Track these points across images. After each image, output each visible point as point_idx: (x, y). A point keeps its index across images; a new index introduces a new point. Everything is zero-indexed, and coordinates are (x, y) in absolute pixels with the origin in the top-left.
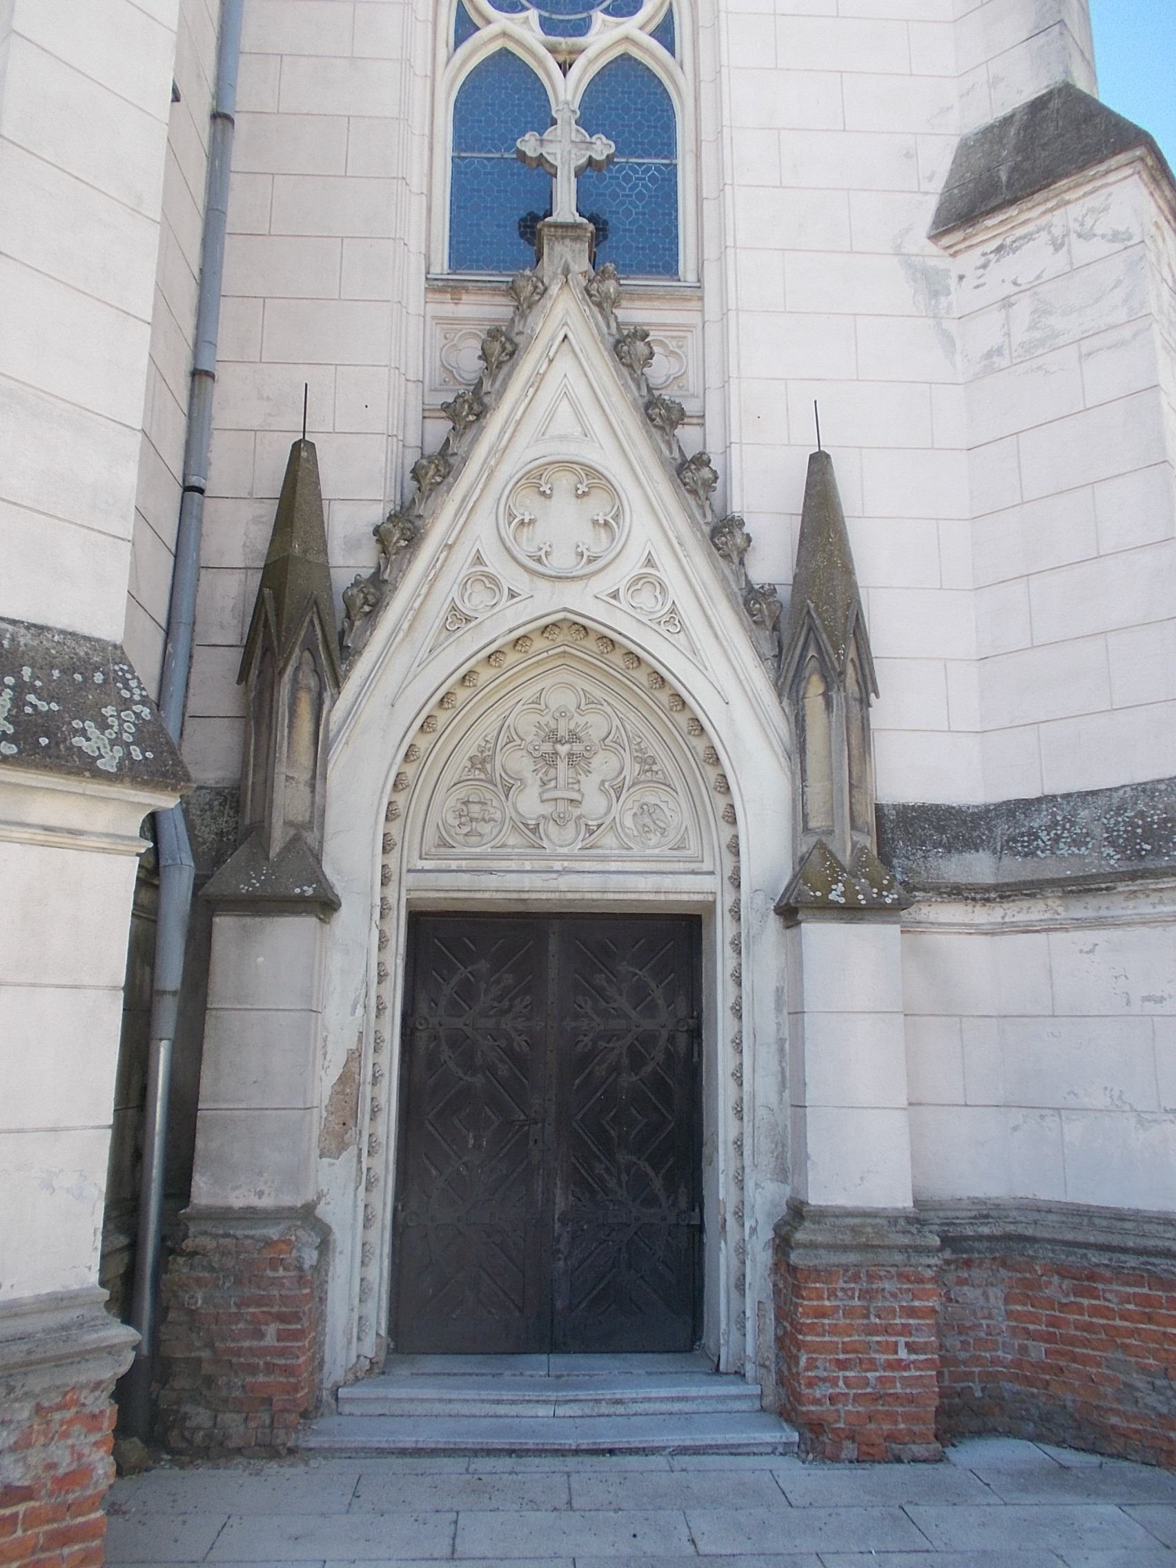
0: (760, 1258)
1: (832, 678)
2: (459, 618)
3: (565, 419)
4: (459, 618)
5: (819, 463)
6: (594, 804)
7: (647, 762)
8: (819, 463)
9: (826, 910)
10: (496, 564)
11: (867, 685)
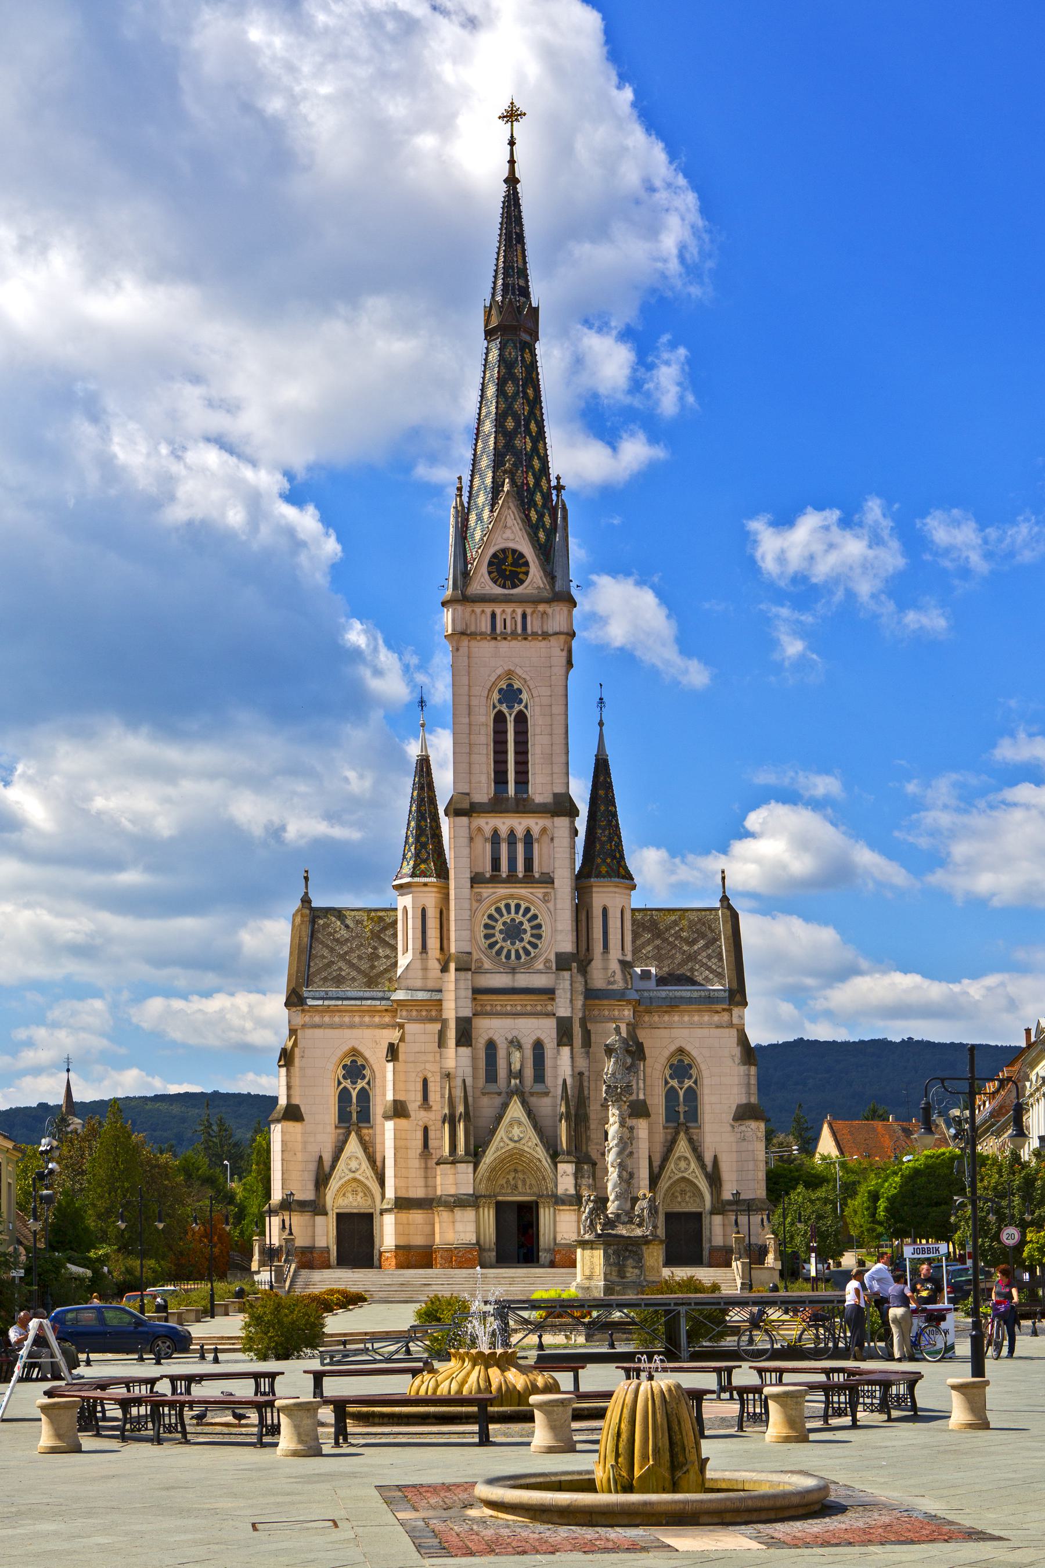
0: (707, 1253)
1: (716, 1186)
2: (670, 1178)
3: (682, 1150)
4: (670, 1178)
5: (715, 1157)
6: (687, 1199)
7: (694, 1194)
8: (715, 1157)
9: (714, 1214)
10: (674, 1170)
11: (721, 1185)
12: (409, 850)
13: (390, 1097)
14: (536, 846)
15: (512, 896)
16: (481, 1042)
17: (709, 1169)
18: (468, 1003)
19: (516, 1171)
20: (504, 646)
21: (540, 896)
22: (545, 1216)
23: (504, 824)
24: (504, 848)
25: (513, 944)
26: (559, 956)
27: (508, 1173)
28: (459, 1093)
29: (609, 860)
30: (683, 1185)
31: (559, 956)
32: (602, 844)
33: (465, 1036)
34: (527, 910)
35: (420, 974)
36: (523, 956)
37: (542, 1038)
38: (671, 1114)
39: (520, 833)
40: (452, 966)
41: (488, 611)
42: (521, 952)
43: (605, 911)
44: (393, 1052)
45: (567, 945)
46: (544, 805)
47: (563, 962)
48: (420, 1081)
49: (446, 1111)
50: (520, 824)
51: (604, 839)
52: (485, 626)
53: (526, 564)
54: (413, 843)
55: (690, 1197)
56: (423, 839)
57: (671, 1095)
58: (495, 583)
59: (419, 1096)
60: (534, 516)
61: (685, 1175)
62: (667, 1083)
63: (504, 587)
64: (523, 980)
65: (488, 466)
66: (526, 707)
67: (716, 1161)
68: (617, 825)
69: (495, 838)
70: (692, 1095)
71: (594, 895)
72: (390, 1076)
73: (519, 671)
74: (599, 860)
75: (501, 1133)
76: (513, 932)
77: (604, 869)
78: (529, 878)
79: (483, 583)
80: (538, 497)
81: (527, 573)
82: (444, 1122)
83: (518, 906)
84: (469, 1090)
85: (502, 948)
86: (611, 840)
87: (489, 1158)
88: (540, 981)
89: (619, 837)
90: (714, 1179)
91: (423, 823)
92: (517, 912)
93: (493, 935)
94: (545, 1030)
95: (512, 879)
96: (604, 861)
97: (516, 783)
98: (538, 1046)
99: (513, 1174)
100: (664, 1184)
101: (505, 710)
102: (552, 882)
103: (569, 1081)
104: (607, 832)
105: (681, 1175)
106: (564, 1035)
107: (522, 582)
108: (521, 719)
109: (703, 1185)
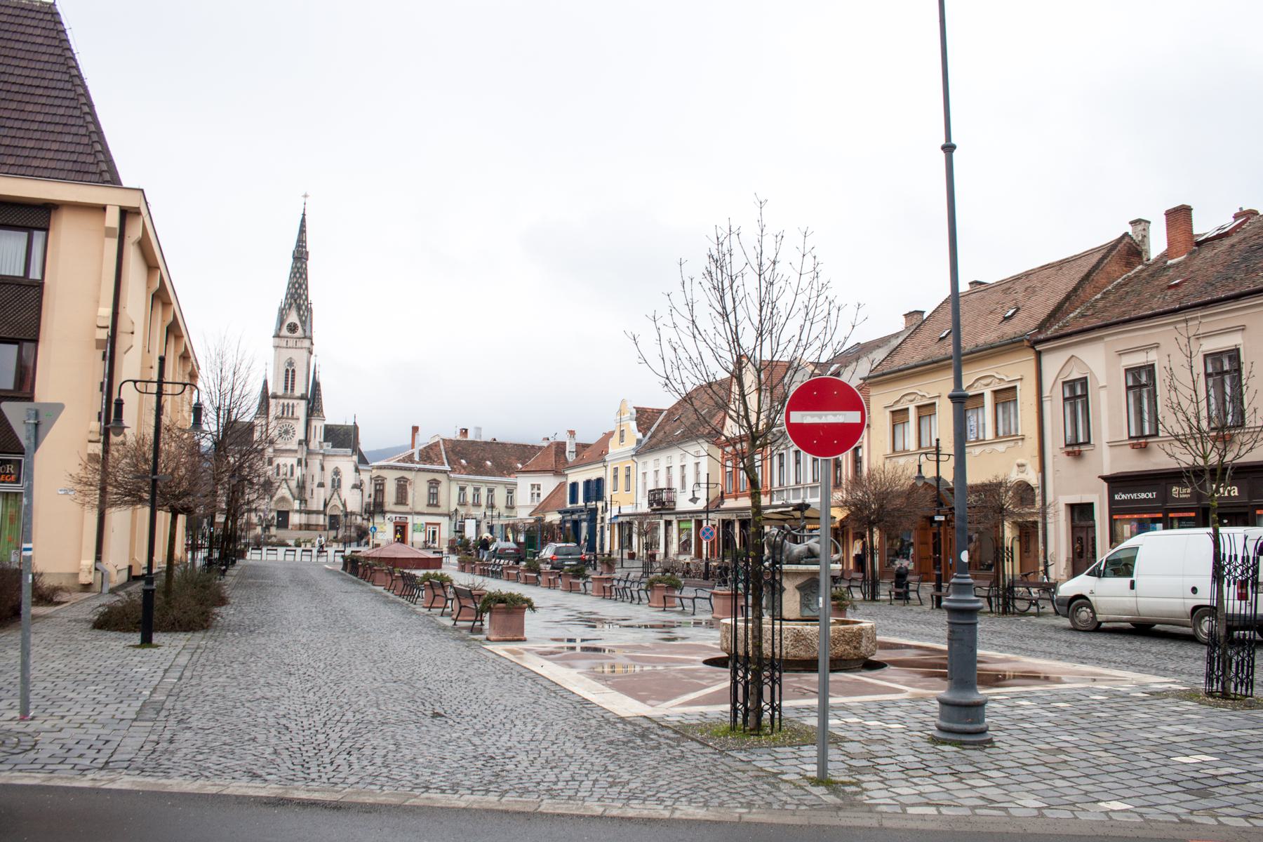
16: (275, 464)
20: (290, 350)
22: (291, 515)
23: (286, 402)
38: (333, 486)
39: (291, 404)
47: (300, 443)
50: (291, 402)
52: (285, 345)
57: (333, 480)
60: (301, 312)
64: (288, 447)
70: (339, 481)
76: (287, 432)
78: (292, 418)
79: (285, 332)
80: (304, 307)
87: (275, 499)
88: (296, 447)
90: (344, 505)
94: (295, 462)
95: (287, 418)
98: (292, 466)
100: (329, 507)
106: (299, 462)
108: (293, 371)
109: (342, 508)
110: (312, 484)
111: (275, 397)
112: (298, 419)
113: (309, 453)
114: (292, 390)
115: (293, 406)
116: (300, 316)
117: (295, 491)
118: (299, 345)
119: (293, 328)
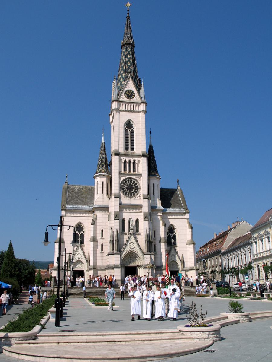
2: (170, 261)
5: (182, 254)
6: (174, 267)
8: (182, 254)
12: (99, 166)
13: (92, 235)
14: (136, 165)
15: (130, 178)
17: (181, 257)
18: (118, 207)
19: (131, 257)
21: (138, 178)
23: (128, 159)
24: (127, 165)
25: (130, 191)
26: (143, 195)
27: (128, 258)
28: (115, 233)
29: (154, 171)
30: (173, 263)
31: (143, 195)
32: (152, 167)
33: (117, 217)
34: (134, 182)
35: (101, 200)
36: (133, 195)
37: (138, 218)
40: (113, 197)
41: (124, 104)
42: (132, 194)
43: (153, 185)
44: (94, 223)
45: (146, 193)
46: (139, 154)
48: (101, 230)
49: (111, 239)
50: (132, 160)
51: (152, 166)
53: (134, 94)
54: (100, 165)
55: (175, 266)
56: (103, 164)
58: (126, 97)
59: (101, 235)
61: (174, 260)
62: (168, 234)
63: (128, 99)
65: (123, 73)
66: (134, 129)
67: (183, 257)
68: (156, 163)
69: (125, 162)
71: (151, 180)
72: (93, 229)
73: (132, 119)
74: (152, 171)
75: (128, 246)
76: (130, 188)
77: (153, 173)
80: (136, 81)
81: (134, 96)
82: (110, 242)
83: (131, 181)
84: (118, 232)
85: (127, 192)
86: (154, 166)
89: (156, 166)
91: (103, 159)
92: (131, 182)
93: (124, 189)
96: (153, 171)
97: (131, 148)
99: (130, 258)
101: (128, 129)
102: (142, 175)
103: (148, 231)
104: (153, 164)
105: (173, 260)
107: (133, 98)
108: (132, 132)
110: (155, 240)
111: (117, 154)
112: (141, 175)
113: (153, 208)
114: (132, 149)
115: (134, 162)
116: (136, 86)
117: (144, 246)
118: (136, 109)
119: (130, 95)
